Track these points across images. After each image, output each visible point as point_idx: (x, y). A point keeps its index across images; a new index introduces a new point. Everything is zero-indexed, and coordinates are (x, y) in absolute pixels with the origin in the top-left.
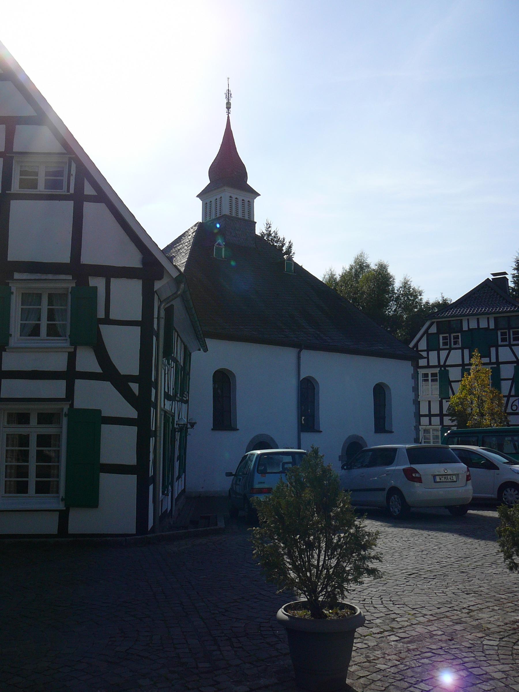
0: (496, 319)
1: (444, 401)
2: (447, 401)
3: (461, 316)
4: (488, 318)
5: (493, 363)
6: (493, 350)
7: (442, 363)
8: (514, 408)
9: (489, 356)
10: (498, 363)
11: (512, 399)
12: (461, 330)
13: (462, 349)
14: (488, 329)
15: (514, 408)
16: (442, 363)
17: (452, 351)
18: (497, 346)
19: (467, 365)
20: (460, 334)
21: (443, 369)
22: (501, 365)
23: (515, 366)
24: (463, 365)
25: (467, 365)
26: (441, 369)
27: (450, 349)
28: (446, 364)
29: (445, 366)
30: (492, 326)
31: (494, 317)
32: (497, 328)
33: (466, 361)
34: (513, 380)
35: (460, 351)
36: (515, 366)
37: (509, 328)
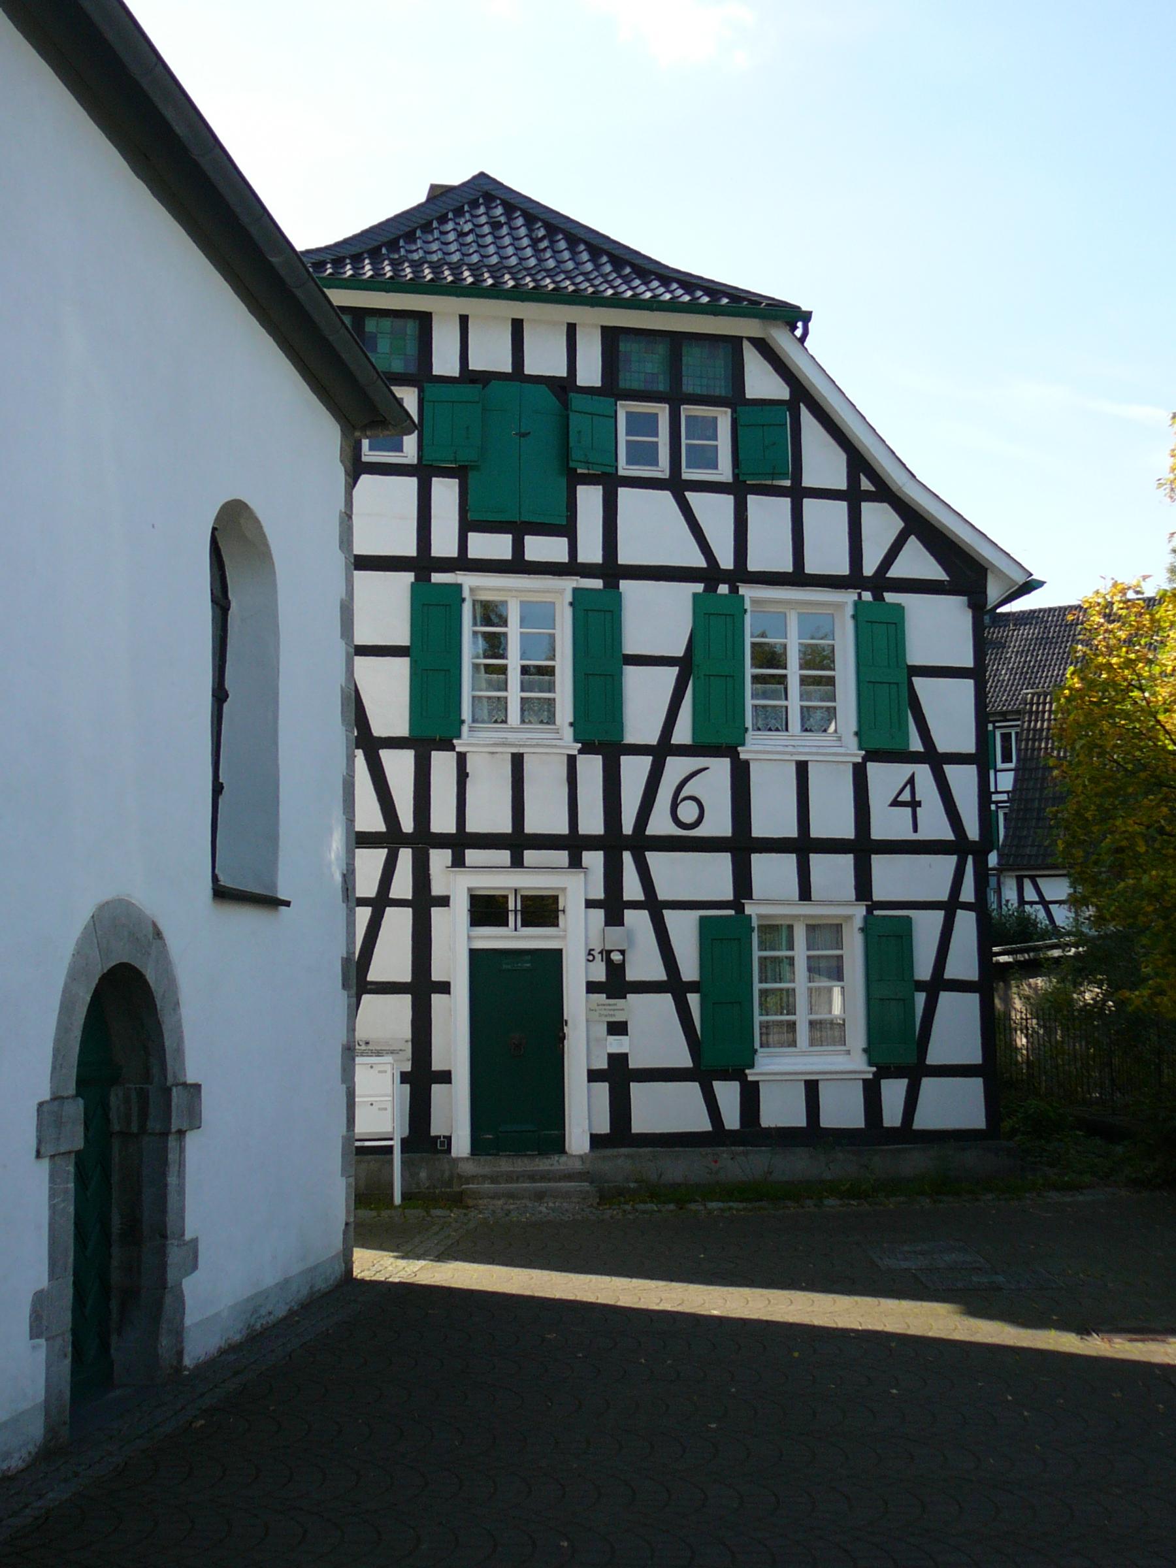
0: (611, 337)
3: (436, 288)
4: (571, 329)
5: (587, 571)
6: (590, 499)
8: (688, 812)
9: (568, 530)
10: (612, 571)
11: (676, 768)
13: (424, 472)
14: (563, 387)
15: (688, 812)
18: (611, 484)
19: (446, 565)
22: (624, 585)
23: (695, 595)
24: (422, 564)
25: (446, 565)
30: (590, 373)
31: (604, 329)
32: (612, 387)
33: (444, 544)
34: (685, 665)
35: (412, 483)
36: (695, 596)
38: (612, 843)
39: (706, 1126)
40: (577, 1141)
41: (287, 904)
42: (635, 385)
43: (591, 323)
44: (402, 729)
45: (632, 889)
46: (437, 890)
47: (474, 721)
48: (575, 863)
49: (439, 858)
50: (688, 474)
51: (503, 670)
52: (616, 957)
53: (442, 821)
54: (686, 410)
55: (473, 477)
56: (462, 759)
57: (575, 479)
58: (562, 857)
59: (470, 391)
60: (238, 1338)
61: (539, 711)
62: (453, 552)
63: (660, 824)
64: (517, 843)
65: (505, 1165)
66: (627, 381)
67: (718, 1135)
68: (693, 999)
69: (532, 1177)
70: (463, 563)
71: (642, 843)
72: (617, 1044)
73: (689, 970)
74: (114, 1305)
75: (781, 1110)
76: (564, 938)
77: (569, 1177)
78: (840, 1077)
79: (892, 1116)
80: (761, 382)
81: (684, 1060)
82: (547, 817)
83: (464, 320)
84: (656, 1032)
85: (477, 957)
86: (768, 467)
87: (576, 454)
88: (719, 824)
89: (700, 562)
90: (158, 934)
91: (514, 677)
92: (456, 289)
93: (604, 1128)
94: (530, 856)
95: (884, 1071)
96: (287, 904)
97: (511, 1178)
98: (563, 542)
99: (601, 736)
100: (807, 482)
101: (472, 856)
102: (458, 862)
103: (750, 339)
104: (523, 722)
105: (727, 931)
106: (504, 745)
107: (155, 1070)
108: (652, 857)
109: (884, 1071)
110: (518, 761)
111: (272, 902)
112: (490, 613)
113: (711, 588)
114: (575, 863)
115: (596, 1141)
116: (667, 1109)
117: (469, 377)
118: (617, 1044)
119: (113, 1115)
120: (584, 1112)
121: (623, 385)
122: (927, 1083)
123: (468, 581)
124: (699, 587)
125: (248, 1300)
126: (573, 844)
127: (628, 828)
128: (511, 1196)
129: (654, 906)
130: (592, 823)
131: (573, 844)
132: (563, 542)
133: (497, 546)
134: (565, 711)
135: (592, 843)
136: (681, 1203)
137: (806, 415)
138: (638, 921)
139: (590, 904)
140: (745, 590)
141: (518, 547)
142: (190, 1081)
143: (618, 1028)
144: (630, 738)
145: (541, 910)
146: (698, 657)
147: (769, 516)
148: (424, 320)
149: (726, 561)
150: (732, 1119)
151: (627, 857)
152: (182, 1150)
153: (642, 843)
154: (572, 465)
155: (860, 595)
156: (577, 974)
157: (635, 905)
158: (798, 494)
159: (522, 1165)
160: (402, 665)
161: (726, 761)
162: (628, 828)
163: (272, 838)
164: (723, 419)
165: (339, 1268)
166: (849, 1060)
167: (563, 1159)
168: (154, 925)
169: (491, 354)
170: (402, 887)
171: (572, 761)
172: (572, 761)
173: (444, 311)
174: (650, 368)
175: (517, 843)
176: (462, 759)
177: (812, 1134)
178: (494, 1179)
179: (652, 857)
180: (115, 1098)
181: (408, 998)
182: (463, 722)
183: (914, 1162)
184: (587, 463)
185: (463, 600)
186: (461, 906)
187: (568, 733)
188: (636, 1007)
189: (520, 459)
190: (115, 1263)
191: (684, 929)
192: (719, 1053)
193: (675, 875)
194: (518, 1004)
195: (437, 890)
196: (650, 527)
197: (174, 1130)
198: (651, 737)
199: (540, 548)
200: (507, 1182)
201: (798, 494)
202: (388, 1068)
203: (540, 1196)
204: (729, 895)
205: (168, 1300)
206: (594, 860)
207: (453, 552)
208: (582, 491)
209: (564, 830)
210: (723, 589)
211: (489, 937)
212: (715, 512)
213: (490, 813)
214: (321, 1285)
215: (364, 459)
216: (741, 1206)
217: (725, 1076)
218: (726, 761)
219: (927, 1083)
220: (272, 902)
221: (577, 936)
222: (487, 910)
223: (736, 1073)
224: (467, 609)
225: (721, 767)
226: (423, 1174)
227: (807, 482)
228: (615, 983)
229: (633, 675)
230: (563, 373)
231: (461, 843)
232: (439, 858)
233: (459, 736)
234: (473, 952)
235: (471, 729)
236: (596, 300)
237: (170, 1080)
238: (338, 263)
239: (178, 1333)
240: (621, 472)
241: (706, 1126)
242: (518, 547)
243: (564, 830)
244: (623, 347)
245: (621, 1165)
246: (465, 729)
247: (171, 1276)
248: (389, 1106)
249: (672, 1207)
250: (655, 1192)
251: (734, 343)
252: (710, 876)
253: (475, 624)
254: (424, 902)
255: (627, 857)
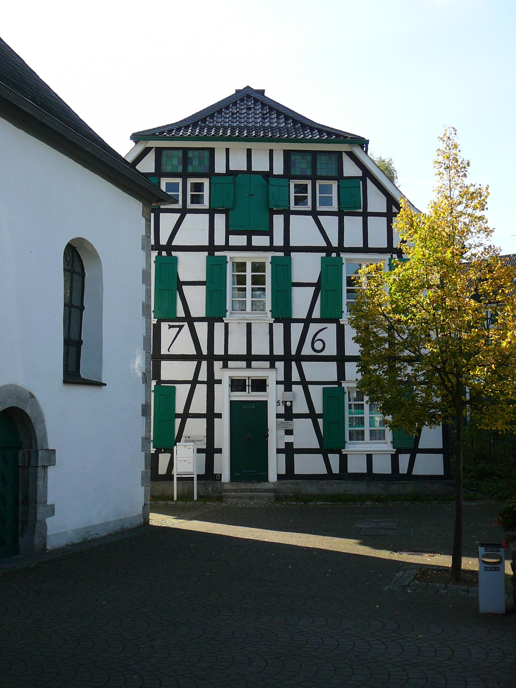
0: (287, 154)
1: (164, 326)
2: (170, 327)
4: (271, 152)
5: (277, 249)
6: (278, 220)
7: (163, 241)
8: (318, 346)
9: (269, 233)
10: (288, 249)
11: (314, 328)
12: (210, 173)
13: (211, 212)
14: (268, 175)
15: (318, 346)
16: (163, 241)
17: (188, 215)
18: (287, 213)
19: (221, 248)
20: (206, 182)
21: (164, 253)
22: (293, 254)
23: (322, 258)
24: (211, 248)
25: (221, 248)
26: (160, 254)
27: (184, 212)
28: (173, 244)
29: (170, 248)
30: (279, 169)
31: (285, 151)
32: (288, 175)
33: (219, 240)
34: (318, 286)
35: (207, 216)
36: (322, 258)
37: (314, 178)
38: (287, 358)
39: (325, 472)
40: (272, 477)
41: (105, 385)
42: (298, 173)
43: (279, 149)
44: (203, 314)
45: (295, 376)
46: (216, 377)
47: (232, 310)
48: (272, 366)
49: (218, 365)
50: (319, 208)
51: (244, 290)
52: (288, 404)
53: (219, 350)
54: (318, 183)
55: (231, 212)
56: (227, 325)
57: (272, 212)
58: (267, 364)
59: (230, 178)
60: (77, 541)
61: (257, 306)
62: (223, 243)
63: (307, 350)
64: (249, 358)
65: (243, 486)
66: (296, 171)
67: (330, 476)
68: (320, 421)
69: (251, 491)
70: (227, 247)
71: (300, 358)
72: (289, 439)
73: (319, 409)
74: (20, 526)
75: (356, 466)
76: (268, 396)
77: (266, 491)
78: (382, 453)
79: (403, 469)
80: (350, 169)
81: (317, 446)
82: (260, 348)
83: (227, 150)
84: (305, 434)
85: (233, 404)
86: (351, 205)
87: (272, 202)
88: (331, 350)
89: (324, 244)
90: (32, 396)
91: (249, 292)
92: (223, 139)
93: (283, 472)
94: (254, 364)
95: (400, 451)
96: (105, 385)
97: (242, 491)
98: (268, 238)
99: (283, 315)
100: (369, 210)
101: (231, 364)
102: (225, 366)
103: (345, 152)
104: (252, 310)
105: (334, 394)
106: (243, 319)
107: (33, 445)
108: (304, 364)
109: (400, 451)
110: (249, 326)
111: (101, 384)
112: (241, 266)
113: (329, 255)
114: (272, 366)
115: (280, 477)
116: (308, 465)
117: (230, 173)
118: (289, 439)
119: (20, 460)
120: (276, 465)
121: (293, 173)
122: (418, 456)
123: (229, 254)
124: (324, 255)
125: (86, 528)
126: (271, 359)
127: (293, 352)
128: (240, 497)
129: (304, 383)
130: (279, 350)
131: (271, 359)
132: (268, 238)
133: (240, 240)
134: (269, 307)
135: (279, 358)
136: (306, 502)
137: (369, 182)
138: (298, 389)
139: (278, 383)
140: (343, 255)
141: (249, 241)
142: (50, 447)
143: (289, 432)
144: (295, 316)
145: (260, 385)
146: (323, 283)
147: (353, 225)
148: (212, 151)
149: (335, 243)
150: (336, 470)
151: (294, 364)
152: (45, 473)
153: (300, 358)
154: (270, 207)
155: (392, 256)
156: (273, 411)
157: (297, 383)
158: (365, 215)
159: (249, 486)
160: (203, 288)
161: (334, 325)
162: (293, 352)
163: (100, 360)
164: (335, 185)
165: (141, 520)
166: (386, 446)
167: (266, 484)
168: (30, 392)
169: (238, 163)
170: (203, 376)
171: (271, 325)
172: (271, 325)
173: (220, 147)
174: (304, 166)
175: (249, 358)
176: (227, 325)
177: (369, 476)
178: (236, 491)
179: (304, 364)
180: (20, 454)
181: (205, 420)
182: (227, 311)
183: (409, 488)
184: (277, 206)
185: (227, 262)
186: (226, 383)
187: (269, 314)
188: (298, 424)
189: (249, 205)
190: (20, 511)
191: (317, 393)
192: (330, 442)
193: (313, 371)
194: (249, 422)
195: (216, 377)
196: (303, 230)
197: (39, 465)
198: (304, 316)
199: (259, 241)
200: (241, 492)
201: (365, 215)
202: (192, 447)
203: (252, 498)
204: (335, 379)
205: (38, 525)
206: (280, 365)
207: (223, 243)
208: (275, 216)
209: (268, 353)
210: (334, 255)
211: (238, 396)
212: (330, 224)
213: (237, 347)
214: (128, 525)
215: (188, 207)
216: (330, 503)
217: (333, 452)
218: (334, 325)
219: (418, 456)
220: (101, 384)
221: (273, 396)
222: (237, 385)
223: (338, 451)
224: (229, 267)
225: (332, 327)
226: (210, 489)
227: (369, 210)
228: (288, 414)
229: (296, 291)
230: (267, 169)
231: (226, 358)
232: (218, 365)
233: (225, 317)
234: (231, 402)
235: (231, 313)
236: (279, 140)
237: (39, 447)
238: (170, 131)
239: (44, 537)
240: (292, 209)
241: (325, 472)
242: (249, 241)
243: (268, 353)
244: (293, 158)
245: (288, 486)
246: (228, 314)
247: (39, 517)
248: (192, 461)
249: (302, 503)
250: (297, 497)
251: (339, 154)
252: (328, 371)
253: (233, 271)
254: (212, 382)
255: (294, 364)
